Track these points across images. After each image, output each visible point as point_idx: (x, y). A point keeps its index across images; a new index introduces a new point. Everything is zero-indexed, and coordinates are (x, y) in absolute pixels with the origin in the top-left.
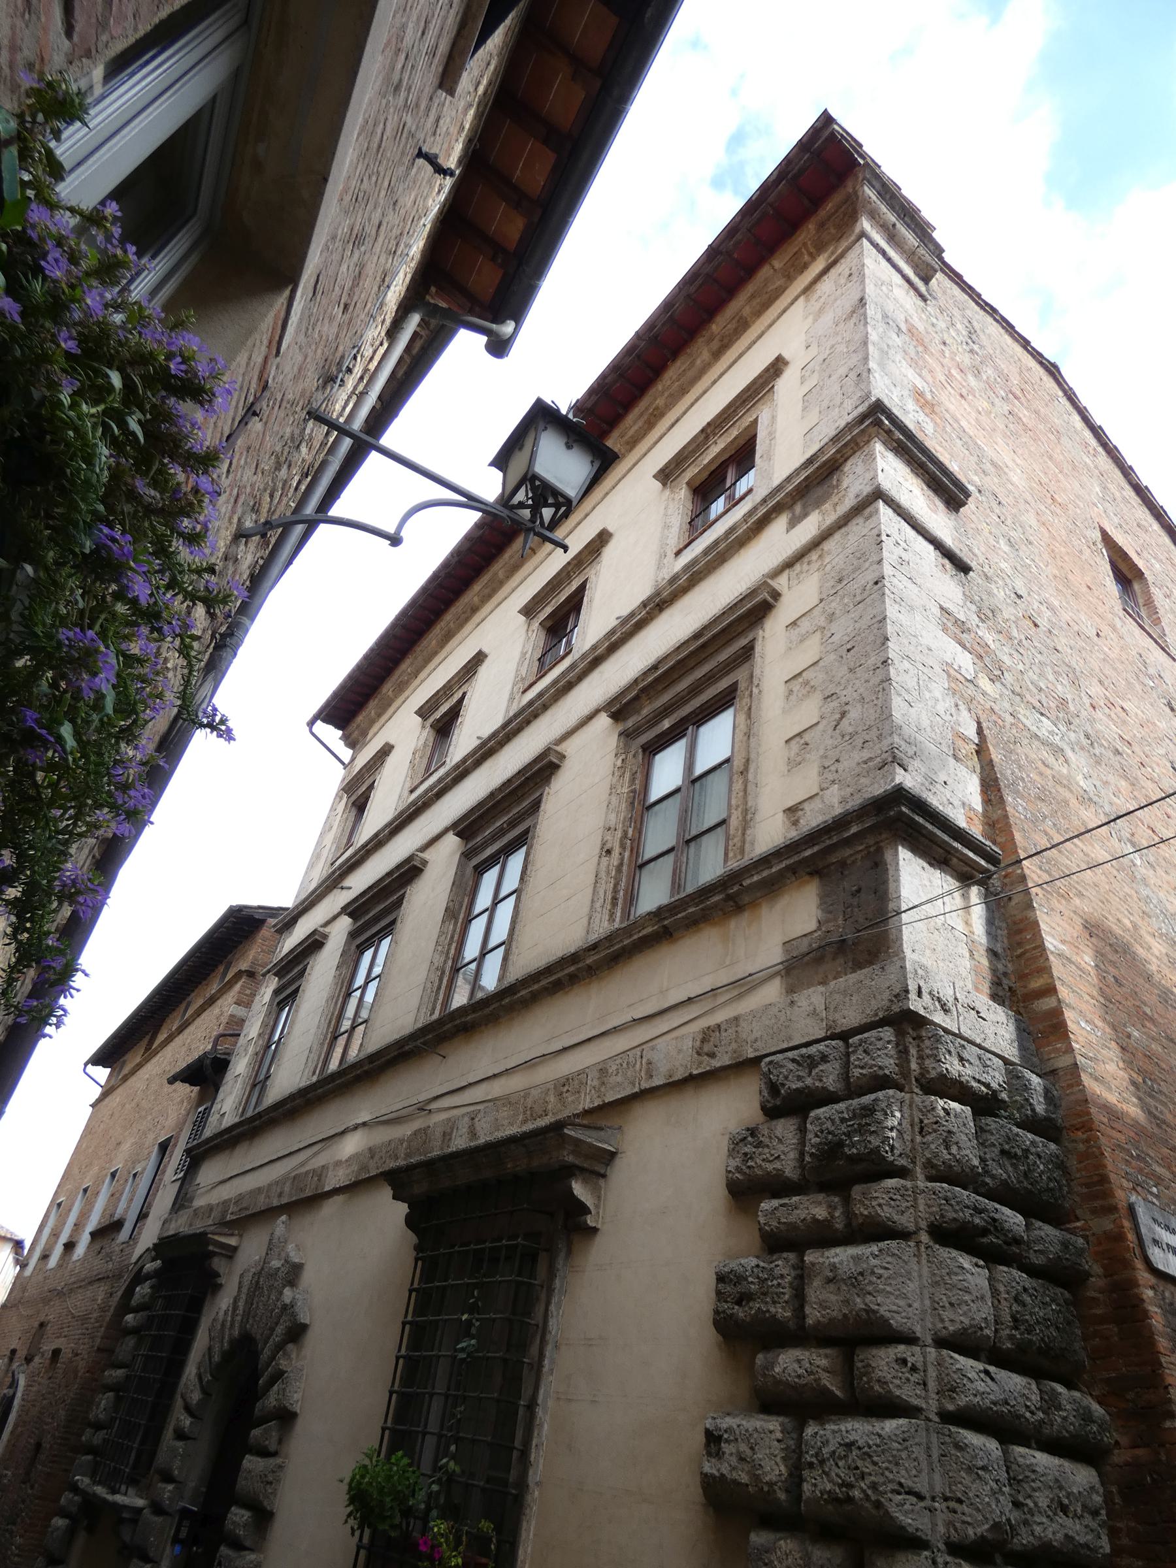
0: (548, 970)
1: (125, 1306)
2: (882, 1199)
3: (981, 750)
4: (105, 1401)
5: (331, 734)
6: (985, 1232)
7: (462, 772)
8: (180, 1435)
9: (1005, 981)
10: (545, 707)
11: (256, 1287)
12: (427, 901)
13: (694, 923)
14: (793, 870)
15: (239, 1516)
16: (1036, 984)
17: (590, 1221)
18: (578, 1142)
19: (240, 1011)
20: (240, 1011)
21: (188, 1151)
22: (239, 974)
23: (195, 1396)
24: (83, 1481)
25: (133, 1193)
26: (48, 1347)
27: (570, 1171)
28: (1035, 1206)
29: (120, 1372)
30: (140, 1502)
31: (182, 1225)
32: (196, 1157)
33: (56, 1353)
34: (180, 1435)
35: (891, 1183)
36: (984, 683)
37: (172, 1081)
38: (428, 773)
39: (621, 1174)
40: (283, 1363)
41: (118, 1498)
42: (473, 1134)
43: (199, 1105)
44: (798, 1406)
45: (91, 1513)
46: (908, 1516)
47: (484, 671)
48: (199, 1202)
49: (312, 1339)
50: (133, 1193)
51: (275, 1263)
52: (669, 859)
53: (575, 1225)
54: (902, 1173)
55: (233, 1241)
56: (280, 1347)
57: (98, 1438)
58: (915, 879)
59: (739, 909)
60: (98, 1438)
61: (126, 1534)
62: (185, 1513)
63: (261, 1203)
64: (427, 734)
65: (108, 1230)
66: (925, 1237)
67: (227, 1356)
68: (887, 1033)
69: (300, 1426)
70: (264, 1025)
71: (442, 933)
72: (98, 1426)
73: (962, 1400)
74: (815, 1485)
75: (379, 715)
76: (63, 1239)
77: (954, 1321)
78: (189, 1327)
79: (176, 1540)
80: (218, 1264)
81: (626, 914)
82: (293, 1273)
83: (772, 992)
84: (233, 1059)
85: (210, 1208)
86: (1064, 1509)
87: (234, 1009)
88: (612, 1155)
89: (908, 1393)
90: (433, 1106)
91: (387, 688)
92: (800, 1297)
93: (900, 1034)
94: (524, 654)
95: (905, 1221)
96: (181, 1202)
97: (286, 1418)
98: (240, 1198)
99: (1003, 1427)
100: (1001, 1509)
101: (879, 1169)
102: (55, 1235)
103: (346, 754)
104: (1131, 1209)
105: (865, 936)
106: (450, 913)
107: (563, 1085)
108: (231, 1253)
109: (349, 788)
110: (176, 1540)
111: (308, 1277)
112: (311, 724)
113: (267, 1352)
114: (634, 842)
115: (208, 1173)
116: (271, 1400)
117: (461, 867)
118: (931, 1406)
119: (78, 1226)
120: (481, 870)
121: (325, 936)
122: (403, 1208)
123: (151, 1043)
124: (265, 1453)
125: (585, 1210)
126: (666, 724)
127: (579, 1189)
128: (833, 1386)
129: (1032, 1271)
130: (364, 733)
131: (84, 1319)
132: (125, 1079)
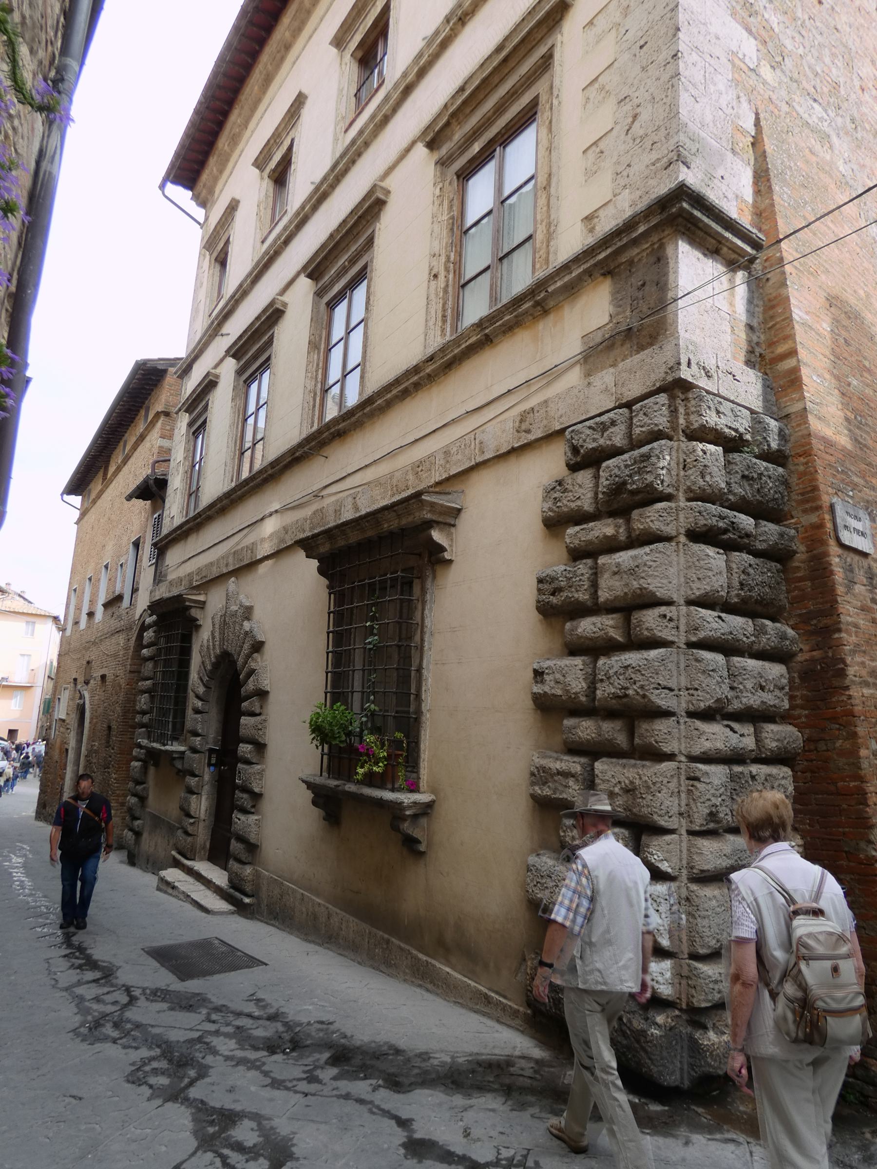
0: (397, 381)
1: (140, 644)
2: (652, 518)
3: (756, 142)
4: (143, 701)
5: (181, 194)
6: (725, 531)
7: (302, 220)
8: (197, 711)
9: (758, 350)
10: (367, 144)
11: (224, 624)
12: (291, 338)
13: (509, 329)
14: (589, 273)
15: (245, 749)
16: (781, 349)
17: (447, 556)
18: (432, 505)
19: (166, 443)
20: (166, 443)
21: (155, 545)
22: (158, 415)
23: (201, 690)
24: (144, 742)
25: (124, 576)
26: (97, 674)
27: (429, 524)
28: (761, 511)
29: (148, 682)
30: (182, 749)
31: (163, 592)
32: (161, 548)
33: (103, 677)
34: (197, 711)
35: (660, 505)
36: (766, 72)
37: (129, 498)
38: (274, 223)
39: (465, 522)
40: (253, 665)
41: (168, 748)
42: (357, 509)
43: (154, 512)
44: (593, 649)
45: (153, 758)
46: (662, 700)
47: (307, 113)
48: (171, 577)
49: (267, 648)
50: (124, 576)
51: (234, 608)
52: (486, 277)
53: (436, 558)
54: (669, 498)
55: (201, 598)
56: (249, 656)
57: (146, 719)
58: (691, 269)
59: (546, 312)
60: (146, 719)
61: (179, 765)
62: (211, 751)
63: (215, 572)
64: (267, 185)
65: (114, 601)
66: (683, 539)
67: (216, 666)
68: (663, 398)
69: (272, 697)
70: (186, 450)
71: (309, 363)
72: (144, 713)
73: (702, 634)
74: (603, 691)
75: (221, 172)
76: (85, 610)
77: (699, 589)
78: (185, 652)
79: (209, 765)
80: (194, 613)
81: (455, 328)
82: (248, 613)
83: (574, 377)
84: (170, 479)
85: (180, 580)
86: (762, 688)
87: (161, 442)
88: (459, 511)
89: (666, 634)
90: (324, 493)
91: (222, 143)
92: (594, 585)
93: (672, 398)
94: (340, 91)
95: (670, 530)
96: (159, 578)
97: (262, 694)
98: (199, 571)
99: (727, 648)
100: (724, 691)
101: (651, 496)
102: (79, 609)
103: (199, 213)
104: (832, 507)
105: (646, 324)
106: (313, 345)
107: (418, 466)
108: (202, 605)
109: (209, 245)
110: (209, 765)
111: (257, 614)
112: (162, 187)
113: (240, 661)
114: (456, 265)
115: (173, 556)
116: (250, 685)
117: (315, 305)
118: (681, 640)
119: (92, 602)
120: (332, 305)
121: (217, 376)
122: (315, 563)
123: (105, 474)
124: (253, 714)
125: (442, 549)
126: (476, 147)
127: (437, 535)
128: (618, 636)
129: (756, 554)
130: (211, 191)
131: (115, 656)
132: (94, 502)
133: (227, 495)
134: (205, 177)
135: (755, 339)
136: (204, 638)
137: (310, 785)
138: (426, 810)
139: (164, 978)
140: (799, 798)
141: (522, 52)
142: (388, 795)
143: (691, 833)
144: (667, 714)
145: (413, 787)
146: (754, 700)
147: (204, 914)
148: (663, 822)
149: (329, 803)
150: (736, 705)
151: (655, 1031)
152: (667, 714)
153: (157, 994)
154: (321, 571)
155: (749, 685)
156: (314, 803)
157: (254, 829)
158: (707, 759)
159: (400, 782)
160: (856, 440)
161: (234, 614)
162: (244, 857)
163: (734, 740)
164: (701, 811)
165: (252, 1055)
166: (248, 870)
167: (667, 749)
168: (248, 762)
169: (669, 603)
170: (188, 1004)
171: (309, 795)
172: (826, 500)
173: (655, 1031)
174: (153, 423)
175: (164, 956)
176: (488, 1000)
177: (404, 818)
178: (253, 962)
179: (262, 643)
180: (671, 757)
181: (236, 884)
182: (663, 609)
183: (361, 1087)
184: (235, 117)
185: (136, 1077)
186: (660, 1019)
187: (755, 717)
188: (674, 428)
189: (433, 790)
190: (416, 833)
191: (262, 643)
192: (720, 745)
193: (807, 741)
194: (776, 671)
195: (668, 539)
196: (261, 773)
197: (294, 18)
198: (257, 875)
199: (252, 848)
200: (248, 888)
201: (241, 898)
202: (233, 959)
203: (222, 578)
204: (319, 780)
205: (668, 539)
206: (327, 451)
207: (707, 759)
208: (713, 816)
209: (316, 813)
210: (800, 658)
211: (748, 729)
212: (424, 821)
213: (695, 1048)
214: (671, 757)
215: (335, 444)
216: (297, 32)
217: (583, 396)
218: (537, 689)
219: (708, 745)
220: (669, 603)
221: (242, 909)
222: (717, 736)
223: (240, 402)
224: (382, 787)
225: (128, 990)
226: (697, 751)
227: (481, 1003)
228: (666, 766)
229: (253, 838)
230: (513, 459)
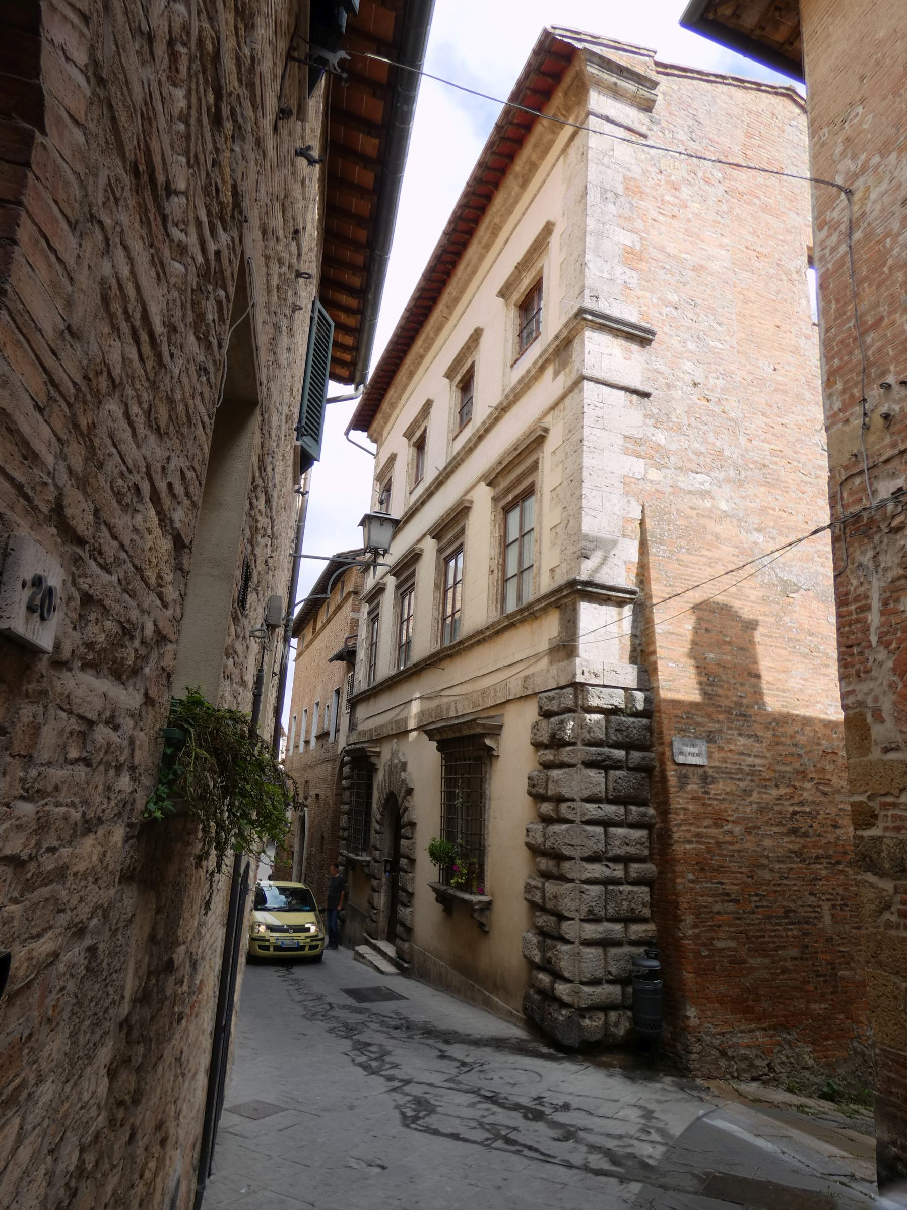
0: (473, 636)
1: (340, 778)
2: (565, 754)
3: (642, 523)
4: (344, 819)
5: (360, 436)
6: (604, 761)
7: (430, 494)
8: (377, 833)
9: (639, 649)
10: (462, 460)
11: (391, 772)
12: (426, 570)
13: (523, 621)
14: (550, 604)
15: (403, 862)
16: (651, 649)
17: (495, 753)
18: (484, 725)
19: (355, 615)
20: (355, 615)
21: (348, 701)
22: (349, 594)
23: (379, 817)
24: (344, 852)
25: (329, 716)
26: (313, 793)
27: (484, 735)
28: (627, 746)
29: (347, 807)
30: (368, 858)
31: (354, 738)
32: (354, 703)
33: (317, 795)
34: (377, 833)
35: (568, 748)
36: (654, 475)
37: (331, 660)
38: (417, 482)
39: (505, 732)
40: (407, 804)
41: (359, 858)
42: (457, 711)
43: (349, 671)
44: (547, 820)
45: (351, 864)
46: (567, 851)
47: (434, 411)
48: (360, 728)
49: (415, 792)
50: (329, 716)
51: (396, 761)
52: (515, 579)
53: (489, 755)
54: (574, 744)
55: (378, 749)
56: (404, 797)
57: (346, 834)
58: (590, 615)
59: (536, 618)
60: (346, 834)
61: (366, 870)
62: (386, 861)
63: (385, 732)
64: (412, 451)
65: (323, 736)
66: (580, 766)
67: (387, 800)
68: (570, 690)
69: (418, 827)
70: (367, 632)
71: (435, 598)
72: (345, 829)
73: (586, 818)
74: (548, 844)
75: (386, 423)
76: (303, 738)
77: (586, 793)
78: (370, 787)
79: (386, 871)
80: (373, 760)
81: (503, 609)
82: (404, 766)
83: (545, 662)
84: (358, 650)
85: (365, 732)
86: (628, 845)
87: (351, 615)
88: (501, 726)
89: (570, 817)
90: (443, 693)
91: (385, 406)
92: (546, 787)
93: (576, 689)
94: (450, 409)
95: (573, 761)
96: (352, 727)
97: (413, 825)
98: (376, 729)
99: (606, 823)
100: (601, 846)
101: (564, 744)
102: (298, 735)
103: (373, 447)
104: (671, 743)
105: (566, 647)
106: (437, 587)
107: (484, 692)
108: (378, 754)
109: (379, 478)
110: (386, 871)
111: (410, 767)
112: (347, 434)
113: (400, 800)
114: (504, 567)
115: (362, 712)
116: (405, 819)
117: (438, 558)
118: (578, 820)
119: (308, 732)
120: (447, 561)
121: (385, 585)
122: (435, 744)
123: (314, 629)
124: (408, 838)
125: (493, 749)
126: (510, 497)
127: (488, 742)
128: (553, 814)
129: (629, 769)
130: (381, 434)
131: (325, 780)
132: (307, 647)
133: (391, 678)
134: (375, 425)
135: (638, 642)
136: (380, 777)
137: (434, 890)
138: (488, 906)
139: (351, 1001)
140: (653, 904)
141: (527, 452)
142: (467, 897)
143: (581, 920)
144: (571, 858)
145: (482, 892)
146: (621, 851)
147: (378, 974)
148: (566, 914)
149: (444, 899)
150: (610, 854)
151: (561, 1018)
152: (571, 858)
153: (345, 1007)
154: (438, 749)
155: (617, 843)
156: (437, 900)
157: (409, 917)
158: (589, 882)
159: (474, 889)
160: (705, 693)
161: (396, 767)
162: (404, 936)
163: (607, 872)
164: (584, 909)
165: (385, 1029)
166: (406, 945)
167: (570, 876)
168: (406, 872)
169: (573, 800)
170: (360, 1011)
171: (434, 895)
172: (667, 739)
173: (561, 1018)
174: (345, 599)
175: (351, 992)
176: (511, 1014)
177: (474, 910)
178: (400, 997)
179: (412, 789)
180: (572, 881)
181: (400, 953)
182: (569, 803)
183: (431, 1042)
184: (391, 393)
185: (331, 1030)
186: (564, 1012)
187: (625, 860)
188: (577, 706)
189: (492, 896)
190: (483, 920)
191: (412, 789)
192: (597, 875)
193: (659, 873)
194: (638, 834)
195: (573, 766)
196: (413, 879)
197: (424, 342)
198: (411, 948)
199: (409, 930)
200: (407, 957)
201: (405, 965)
202: (391, 996)
203: (389, 737)
204: (437, 886)
205: (573, 766)
206: (444, 664)
207: (589, 882)
208: (590, 911)
209: (439, 907)
210: (657, 826)
211: (621, 866)
212: (487, 912)
213: (580, 1028)
214: (572, 881)
215: (448, 661)
216: (428, 349)
217: (546, 675)
218: (528, 840)
219: (589, 875)
220: (573, 800)
221: (404, 972)
222: (596, 870)
223: (398, 610)
224: (466, 891)
225: (330, 1005)
226: (583, 878)
227: (508, 1017)
228: (569, 885)
229: (408, 923)
230: (522, 702)
